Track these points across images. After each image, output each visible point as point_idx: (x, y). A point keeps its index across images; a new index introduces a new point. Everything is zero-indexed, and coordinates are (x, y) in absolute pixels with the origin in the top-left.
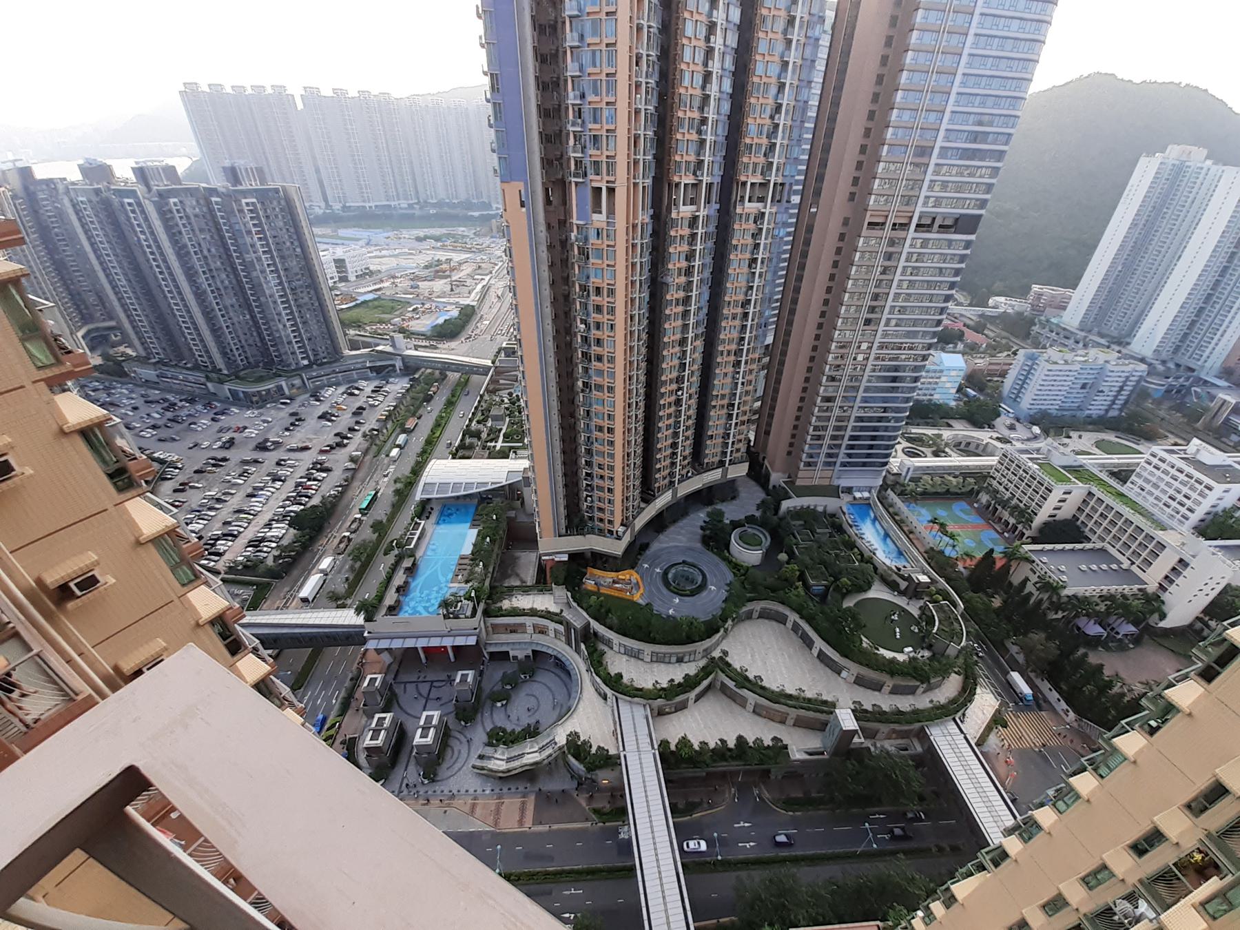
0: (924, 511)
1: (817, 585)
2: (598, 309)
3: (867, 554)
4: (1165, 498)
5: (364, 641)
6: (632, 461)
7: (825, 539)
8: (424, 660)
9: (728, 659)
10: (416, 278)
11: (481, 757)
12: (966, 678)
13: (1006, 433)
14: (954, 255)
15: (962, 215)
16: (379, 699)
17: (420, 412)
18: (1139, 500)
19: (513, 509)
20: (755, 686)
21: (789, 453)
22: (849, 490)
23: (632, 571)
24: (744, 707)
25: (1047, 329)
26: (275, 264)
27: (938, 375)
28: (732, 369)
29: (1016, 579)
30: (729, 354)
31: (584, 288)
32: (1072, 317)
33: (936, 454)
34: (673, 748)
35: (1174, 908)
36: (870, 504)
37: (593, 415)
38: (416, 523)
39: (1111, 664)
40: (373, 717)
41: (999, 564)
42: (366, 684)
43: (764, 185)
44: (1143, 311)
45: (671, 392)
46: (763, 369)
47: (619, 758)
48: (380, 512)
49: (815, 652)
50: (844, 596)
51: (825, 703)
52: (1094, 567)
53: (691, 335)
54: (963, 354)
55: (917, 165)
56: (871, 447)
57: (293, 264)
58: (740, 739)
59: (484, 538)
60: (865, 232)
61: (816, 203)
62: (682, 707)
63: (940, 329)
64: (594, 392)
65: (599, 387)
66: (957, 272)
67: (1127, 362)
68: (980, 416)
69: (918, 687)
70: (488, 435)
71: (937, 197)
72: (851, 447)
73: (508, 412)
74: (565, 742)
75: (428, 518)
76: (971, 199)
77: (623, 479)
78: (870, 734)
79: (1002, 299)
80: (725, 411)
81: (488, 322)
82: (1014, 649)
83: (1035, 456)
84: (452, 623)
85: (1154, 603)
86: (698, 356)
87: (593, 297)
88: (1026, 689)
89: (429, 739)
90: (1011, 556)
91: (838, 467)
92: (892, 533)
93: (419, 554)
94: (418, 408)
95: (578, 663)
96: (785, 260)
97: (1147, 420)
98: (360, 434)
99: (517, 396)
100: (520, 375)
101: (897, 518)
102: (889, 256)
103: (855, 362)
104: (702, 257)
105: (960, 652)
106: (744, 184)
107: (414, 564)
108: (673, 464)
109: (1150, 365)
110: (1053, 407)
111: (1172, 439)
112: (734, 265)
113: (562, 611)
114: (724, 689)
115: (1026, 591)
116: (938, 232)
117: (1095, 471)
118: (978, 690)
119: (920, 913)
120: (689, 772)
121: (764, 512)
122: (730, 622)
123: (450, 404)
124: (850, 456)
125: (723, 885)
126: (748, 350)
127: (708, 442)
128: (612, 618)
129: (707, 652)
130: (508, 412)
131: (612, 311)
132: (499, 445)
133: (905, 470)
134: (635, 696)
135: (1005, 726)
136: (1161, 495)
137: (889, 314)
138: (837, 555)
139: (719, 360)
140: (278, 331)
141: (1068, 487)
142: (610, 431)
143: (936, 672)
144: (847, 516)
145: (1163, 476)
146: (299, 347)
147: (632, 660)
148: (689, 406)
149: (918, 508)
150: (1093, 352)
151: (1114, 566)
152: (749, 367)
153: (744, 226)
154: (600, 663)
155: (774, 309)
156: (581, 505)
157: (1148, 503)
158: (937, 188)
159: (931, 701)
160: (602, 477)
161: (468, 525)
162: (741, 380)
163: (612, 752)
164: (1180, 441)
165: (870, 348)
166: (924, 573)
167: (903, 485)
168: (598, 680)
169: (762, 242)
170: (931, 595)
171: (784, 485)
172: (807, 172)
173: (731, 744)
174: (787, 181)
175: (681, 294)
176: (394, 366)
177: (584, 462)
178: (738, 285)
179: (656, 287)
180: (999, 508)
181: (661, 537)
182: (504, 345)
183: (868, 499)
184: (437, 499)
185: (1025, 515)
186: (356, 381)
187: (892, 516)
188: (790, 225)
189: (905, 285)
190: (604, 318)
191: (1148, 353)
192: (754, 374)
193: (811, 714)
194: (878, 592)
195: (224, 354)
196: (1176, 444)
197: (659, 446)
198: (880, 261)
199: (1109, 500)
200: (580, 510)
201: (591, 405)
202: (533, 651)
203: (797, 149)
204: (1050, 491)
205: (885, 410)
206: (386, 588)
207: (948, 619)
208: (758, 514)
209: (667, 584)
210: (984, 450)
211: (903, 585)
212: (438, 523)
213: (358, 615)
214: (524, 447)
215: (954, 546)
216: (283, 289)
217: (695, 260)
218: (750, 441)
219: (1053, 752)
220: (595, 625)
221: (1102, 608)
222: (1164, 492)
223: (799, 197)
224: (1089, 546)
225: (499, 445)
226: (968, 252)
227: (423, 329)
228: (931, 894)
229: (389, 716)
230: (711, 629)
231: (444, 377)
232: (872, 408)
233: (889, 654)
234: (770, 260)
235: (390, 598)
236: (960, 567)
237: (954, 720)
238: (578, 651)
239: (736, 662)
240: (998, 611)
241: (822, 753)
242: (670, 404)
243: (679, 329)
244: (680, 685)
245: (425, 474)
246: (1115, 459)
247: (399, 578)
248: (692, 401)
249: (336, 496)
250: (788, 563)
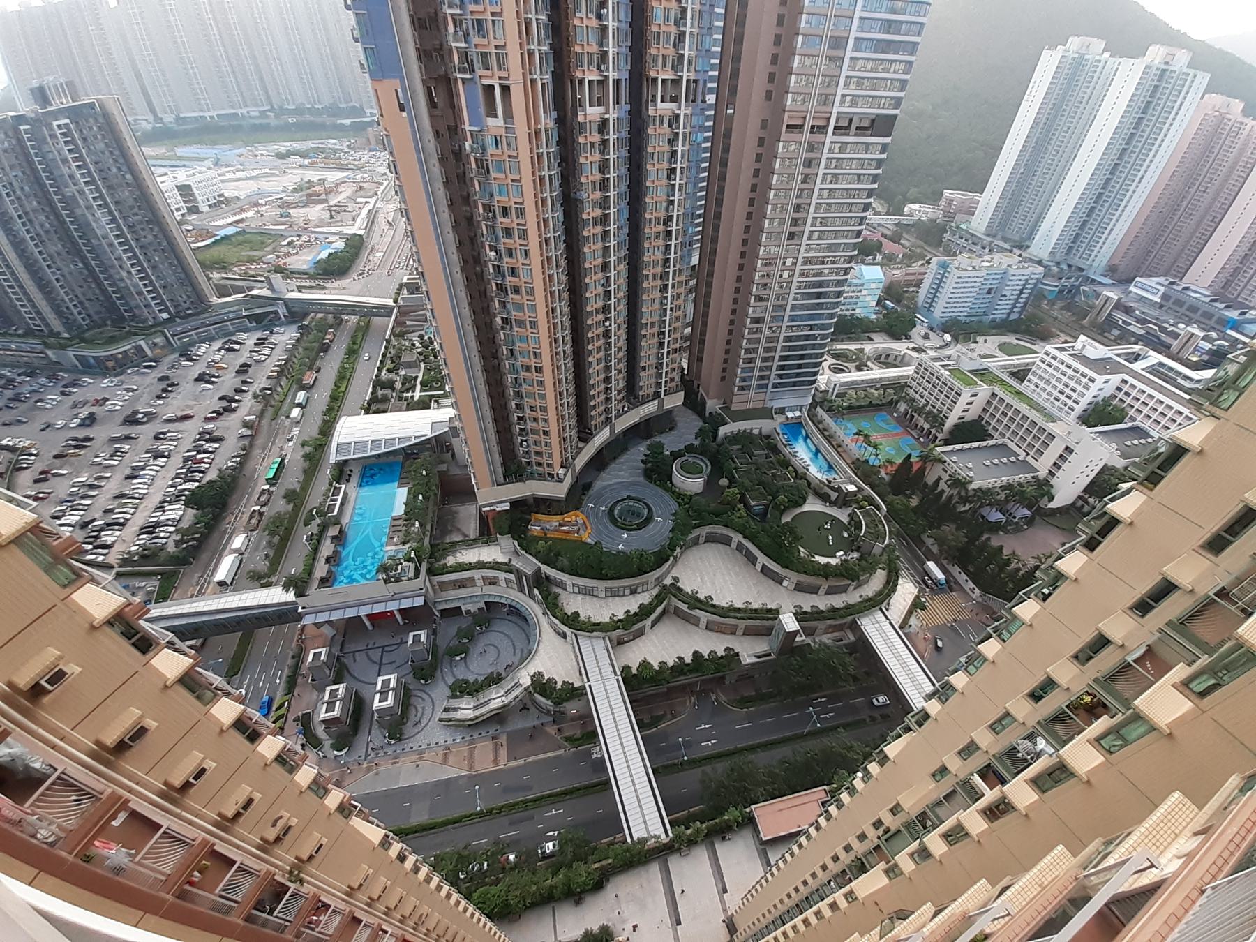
0: (849, 425)
1: (756, 505)
2: (508, 233)
3: (801, 471)
4: (1056, 393)
5: (300, 617)
6: (565, 400)
7: (762, 460)
8: (370, 628)
9: (679, 584)
10: (284, 205)
11: (447, 710)
12: (890, 572)
13: (921, 342)
14: (872, 160)
15: (878, 115)
16: (328, 672)
17: (318, 364)
18: (1034, 397)
19: (444, 462)
20: (707, 605)
21: (723, 379)
22: (782, 411)
23: (577, 512)
24: (698, 626)
25: (957, 236)
26: (101, 197)
27: (859, 288)
28: (659, 295)
29: (930, 480)
30: (654, 278)
31: (488, 208)
32: (979, 223)
33: (859, 369)
34: (634, 671)
35: (1071, 743)
37: (517, 353)
38: (335, 488)
39: (1008, 544)
40: (324, 691)
41: (915, 468)
42: (310, 659)
43: (676, 82)
44: (1041, 214)
45: (598, 324)
46: (691, 292)
47: (585, 689)
48: (292, 480)
49: (759, 567)
50: (782, 513)
51: (770, 611)
52: (996, 461)
53: (613, 259)
54: (882, 265)
55: (831, 59)
56: (800, 366)
57: (125, 194)
58: (696, 655)
59: (416, 497)
60: (784, 136)
61: (732, 103)
62: (641, 633)
63: (860, 240)
64: (516, 329)
65: (521, 323)
66: (875, 178)
67: (1026, 265)
68: (898, 327)
69: (849, 585)
70: (403, 384)
71: (853, 96)
72: (781, 368)
73: (422, 358)
74: (529, 683)
75: (348, 481)
76: (886, 97)
77: (558, 420)
78: (809, 632)
79: (916, 206)
80: (656, 340)
81: (382, 254)
82: (929, 541)
83: (947, 363)
84: (394, 587)
85: (1044, 487)
86: (623, 281)
87: (500, 219)
88: (940, 575)
89: (389, 702)
90: (926, 459)
91: (770, 389)
92: (822, 449)
93: (345, 520)
94: (314, 361)
95: (533, 608)
96: (704, 170)
97: (1042, 320)
98: (249, 396)
99: (429, 338)
100: (429, 315)
101: (826, 433)
102: (809, 163)
103: (781, 280)
104: (617, 168)
105: (884, 549)
106: (655, 80)
107: (341, 532)
108: (608, 400)
109: (1046, 267)
110: (962, 316)
111: (1063, 337)
112: (652, 176)
113: (510, 560)
114: (677, 612)
115: (939, 489)
116: (856, 135)
117: (998, 373)
118: (900, 581)
119: (859, 774)
120: (650, 690)
121: (704, 440)
122: (678, 550)
123: (353, 353)
124: (780, 376)
125: (690, 780)
126: (674, 272)
127: (642, 374)
128: (564, 561)
129: (659, 580)
130: (422, 358)
131: (523, 234)
132: (417, 394)
134: (593, 631)
135: (923, 608)
136: (1052, 390)
137: (812, 226)
138: (773, 475)
139: (645, 285)
140: (122, 280)
141: (973, 390)
142: (539, 370)
143: (864, 570)
145: (1054, 372)
146: (153, 298)
147: (587, 597)
148: (619, 337)
149: (844, 422)
150: (997, 257)
151: (1013, 459)
152: (676, 291)
153: (658, 131)
154: (556, 605)
155: (698, 225)
156: (517, 451)
157: (1041, 399)
158: (852, 86)
159: (861, 596)
160: (535, 420)
161: (396, 484)
162: (669, 307)
163: (577, 684)
164: (1069, 339)
165: (795, 264)
166: (852, 483)
167: (831, 401)
168: (556, 621)
169: (680, 149)
170: (857, 502)
171: (719, 411)
172: (720, 68)
173: (688, 660)
174: (701, 77)
175: (598, 212)
176: (276, 312)
177: (514, 406)
178: (658, 199)
179: (570, 204)
180: (916, 415)
181: (603, 475)
182: (405, 280)
183: (800, 417)
184: (354, 459)
185: (937, 420)
186: (233, 334)
187: (822, 432)
188: (707, 129)
189: (826, 193)
190: (516, 242)
191: (1044, 255)
192: (682, 298)
193: (758, 622)
194: (812, 505)
195: (59, 313)
196: (1066, 342)
197: (591, 382)
198: (800, 169)
199: (1009, 399)
200: (515, 456)
201: (513, 343)
202: (486, 603)
203: (708, 38)
204: (959, 395)
205: (812, 327)
206: (314, 560)
207: (874, 522)
208: (697, 443)
209: (614, 521)
210: (902, 361)
211: (834, 495)
212: (361, 486)
213: (287, 591)
214: (446, 395)
215: (877, 455)
216: (119, 227)
217: (609, 173)
218: (683, 369)
219: (962, 624)
220: (546, 570)
221: (1002, 496)
222: (1055, 387)
223: (714, 96)
224: (992, 442)
225: (417, 394)
226: (884, 156)
227: (305, 267)
228: (867, 757)
229: (341, 687)
230: (661, 558)
231: (339, 323)
232: (799, 326)
233: (823, 560)
234: (689, 169)
235: (321, 570)
236: (883, 474)
238: (532, 596)
239: (687, 586)
240: (915, 510)
241: (770, 655)
242: (598, 336)
243: (600, 253)
244: (636, 614)
245: (336, 434)
246: (1016, 360)
247: (327, 549)
248: (621, 331)
249: (235, 468)
250: (729, 487)
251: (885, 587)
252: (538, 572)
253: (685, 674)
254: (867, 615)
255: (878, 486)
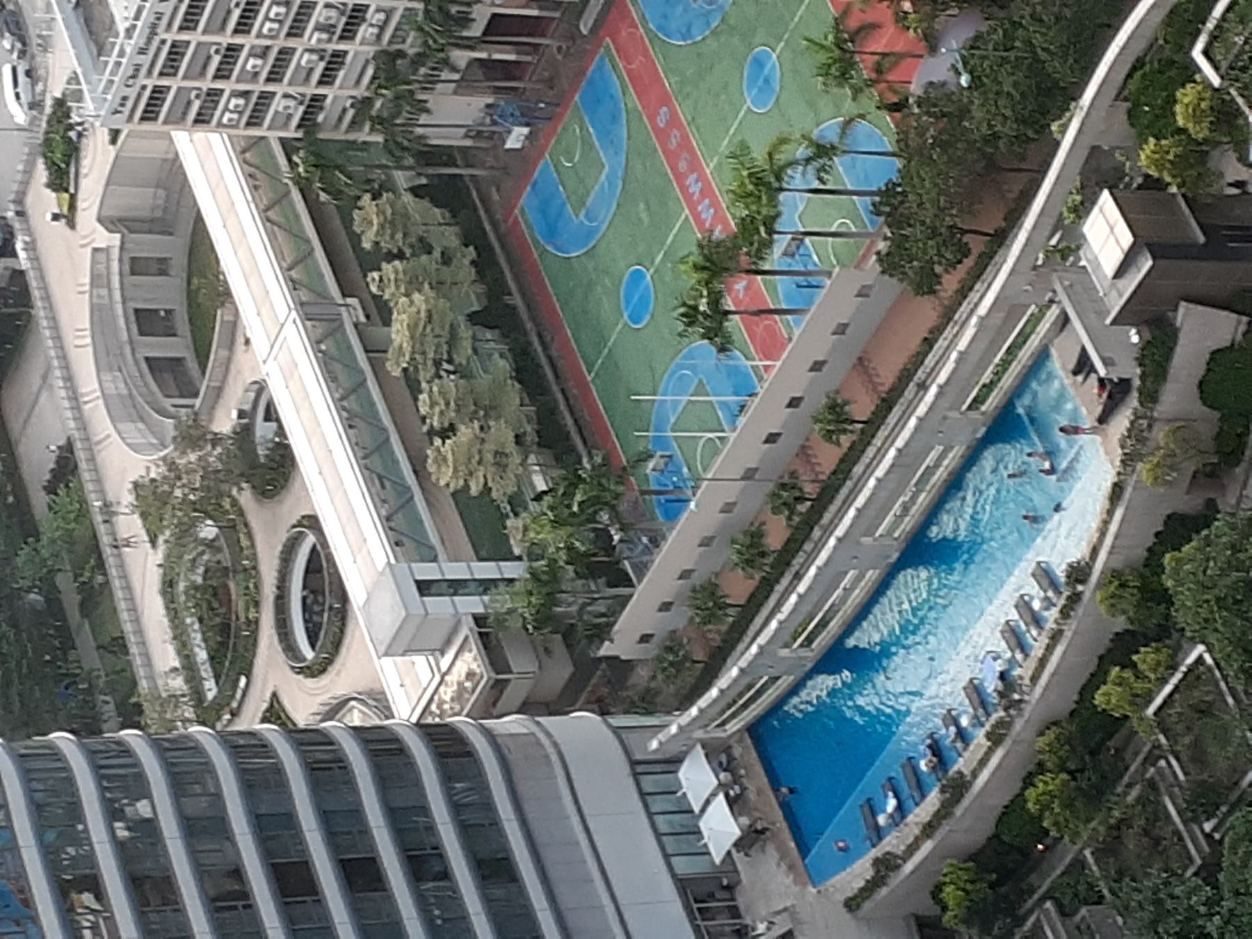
36: (753, 729)
101: (776, 534)
133: (439, 605)
144: (892, 843)
183: (722, 758)
255: (1036, 67)
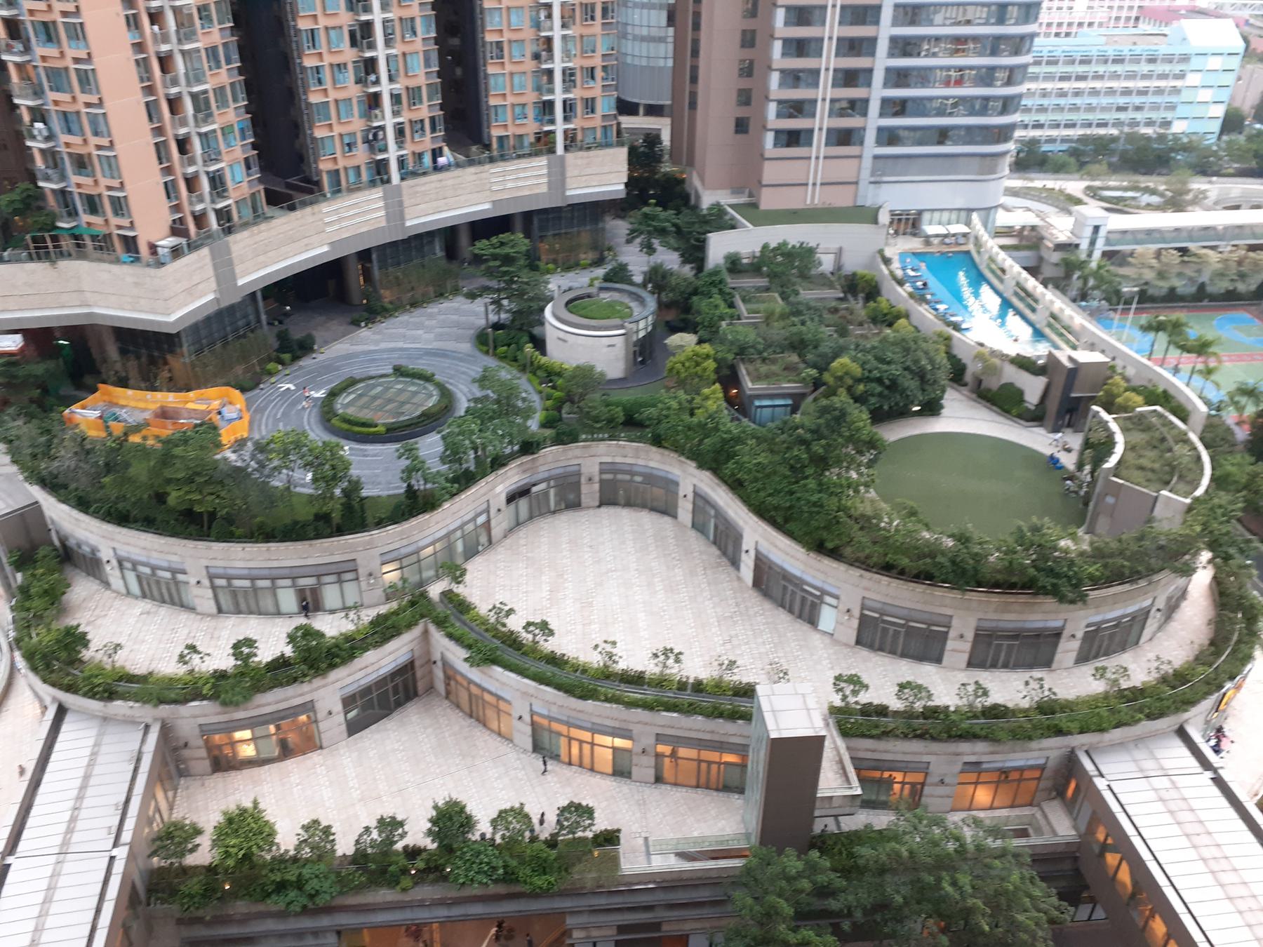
237: (1182, 733)
251: (1199, 659)
252: (31, 517)
253: (393, 882)
254: (1121, 745)
